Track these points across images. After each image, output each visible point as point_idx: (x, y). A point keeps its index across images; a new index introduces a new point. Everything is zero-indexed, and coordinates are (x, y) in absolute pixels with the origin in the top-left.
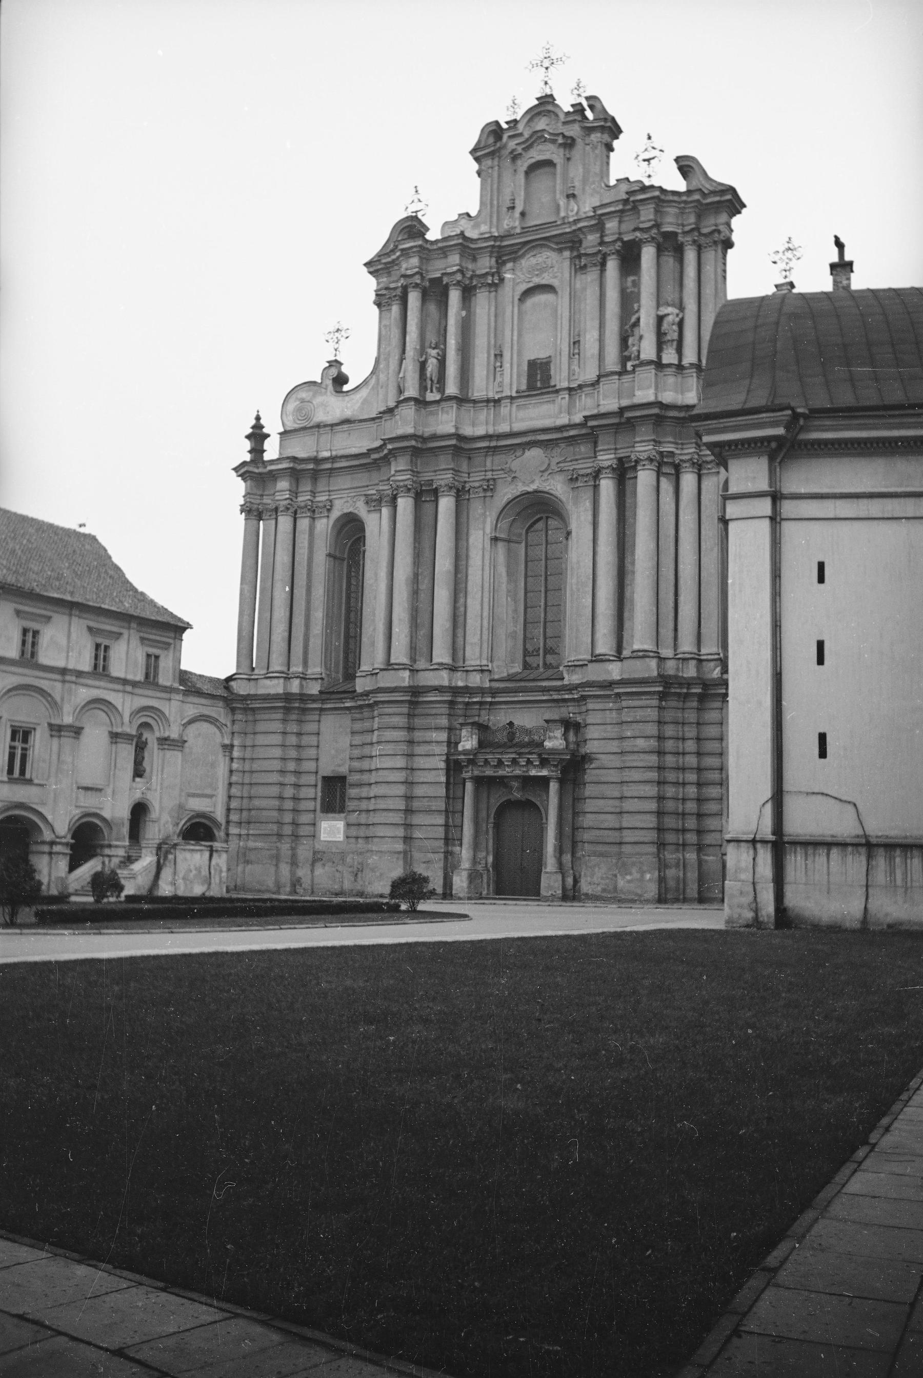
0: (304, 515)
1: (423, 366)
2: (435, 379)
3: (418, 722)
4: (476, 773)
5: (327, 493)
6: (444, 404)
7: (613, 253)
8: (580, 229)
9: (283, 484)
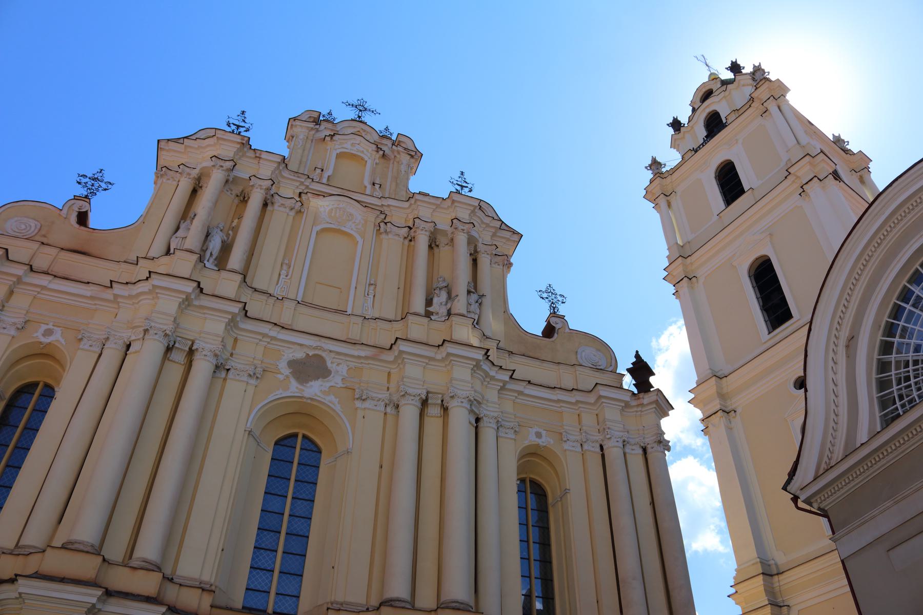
2: (215, 254)
7: (426, 231)
8: (389, 206)
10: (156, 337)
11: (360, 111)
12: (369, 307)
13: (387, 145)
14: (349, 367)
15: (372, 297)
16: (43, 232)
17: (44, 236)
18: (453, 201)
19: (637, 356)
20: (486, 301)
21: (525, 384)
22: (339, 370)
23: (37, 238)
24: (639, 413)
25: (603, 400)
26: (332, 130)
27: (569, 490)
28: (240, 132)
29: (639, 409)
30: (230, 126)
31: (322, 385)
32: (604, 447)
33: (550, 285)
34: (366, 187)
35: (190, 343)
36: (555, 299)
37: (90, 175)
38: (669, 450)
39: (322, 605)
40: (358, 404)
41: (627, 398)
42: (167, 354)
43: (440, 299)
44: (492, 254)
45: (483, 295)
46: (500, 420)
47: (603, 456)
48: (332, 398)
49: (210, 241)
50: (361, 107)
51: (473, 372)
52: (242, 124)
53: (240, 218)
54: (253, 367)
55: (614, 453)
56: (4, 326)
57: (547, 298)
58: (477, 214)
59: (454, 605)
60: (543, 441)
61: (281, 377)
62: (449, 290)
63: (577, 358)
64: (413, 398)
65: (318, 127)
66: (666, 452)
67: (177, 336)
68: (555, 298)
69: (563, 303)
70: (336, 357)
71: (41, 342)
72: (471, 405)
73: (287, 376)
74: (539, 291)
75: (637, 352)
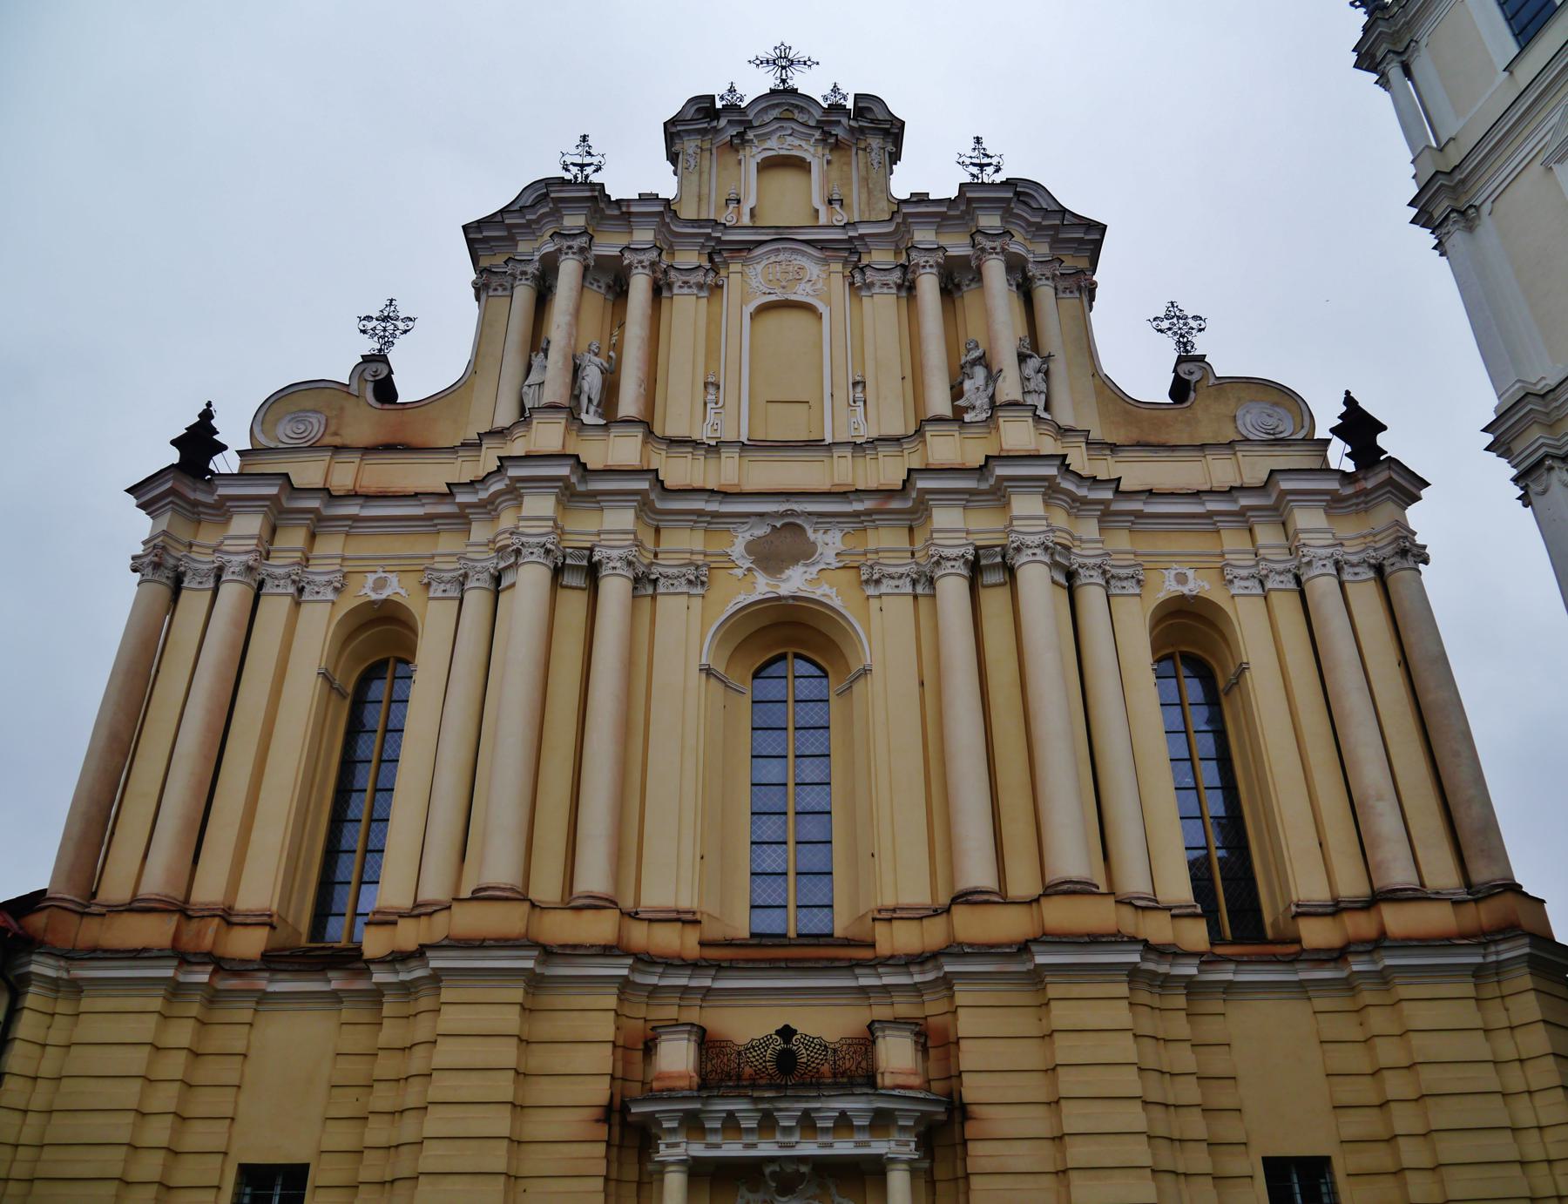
0: (279, 590)
1: (576, 371)
3: (546, 1027)
4: (698, 1150)
5: (339, 561)
6: (614, 431)
7: (931, 266)
8: (862, 237)
9: (248, 525)
10: (533, 558)
11: (783, 68)
12: (860, 422)
13: (840, 121)
14: (844, 532)
15: (862, 404)
16: (332, 428)
17: (336, 434)
18: (970, 200)
19: (1349, 400)
20: (1058, 368)
21: (1143, 497)
22: (830, 543)
23: (328, 440)
24: (1362, 506)
25: (1289, 498)
26: (741, 122)
27: (1248, 663)
28: (587, 177)
29: (1362, 499)
30: (569, 171)
31: (806, 572)
32: (1303, 579)
33: (1172, 303)
34: (817, 211)
35: (587, 553)
36: (1185, 327)
37: (375, 314)
38: (1426, 561)
39: (864, 916)
40: (871, 591)
41: (1333, 485)
42: (557, 579)
43: (974, 385)
44: (1054, 276)
45: (1049, 356)
46: (1108, 568)
47: (1302, 594)
48: (825, 589)
49: (583, 379)
50: (783, 61)
51: (1047, 497)
52: (588, 160)
53: (622, 325)
54: (693, 568)
55: (1323, 587)
56: (317, 589)
57: (1169, 329)
58: (1015, 211)
59: (1065, 887)
61: (739, 572)
62: (983, 360)
63: (1236, 427)
64: (953, 563)
65: (715, 123)
66: (1421, 566)
67: (565, 548)
68: (1185, 324)
69: (1200, 330)
70: (820, 520)
71: (374, 602)
72: (1052, 555)
73: (749, 569)
74: (1155, 320)
75: (1348, 393)
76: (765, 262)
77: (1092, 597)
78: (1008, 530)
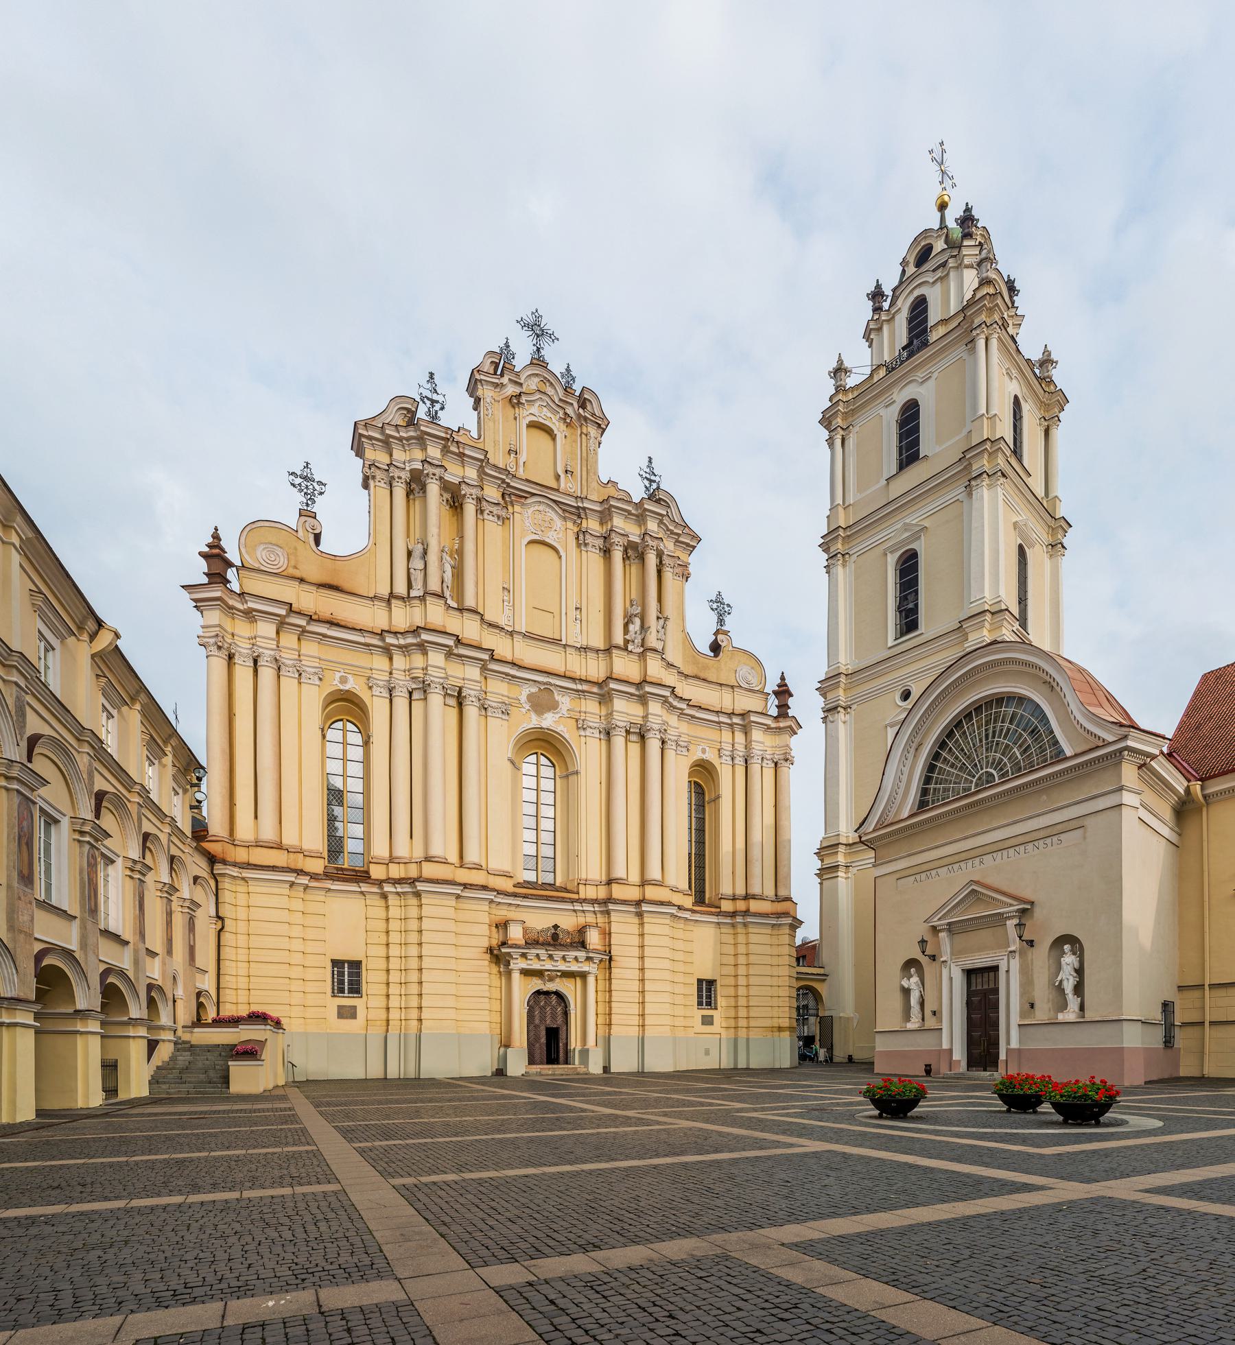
8: (584, 509)
60: (707, 756)
76: (532, 509)
77: (670, 754)
78: (645, 717)
